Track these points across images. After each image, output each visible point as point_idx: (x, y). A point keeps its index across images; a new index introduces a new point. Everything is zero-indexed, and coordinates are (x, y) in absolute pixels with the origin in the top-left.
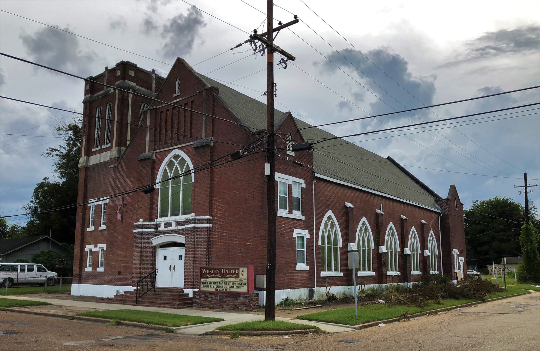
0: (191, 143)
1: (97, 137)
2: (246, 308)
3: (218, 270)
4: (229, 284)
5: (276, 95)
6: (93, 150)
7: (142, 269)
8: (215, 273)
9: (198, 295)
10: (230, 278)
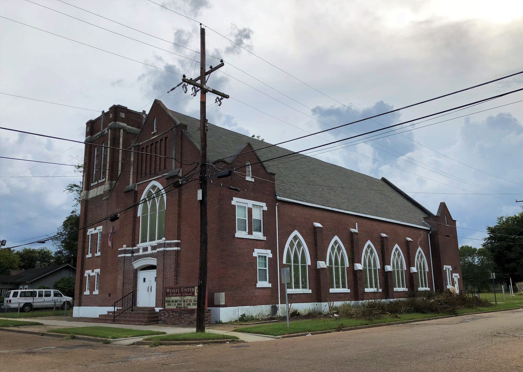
1: (95, 174)
6: (92, 185)
10: (188, 296)
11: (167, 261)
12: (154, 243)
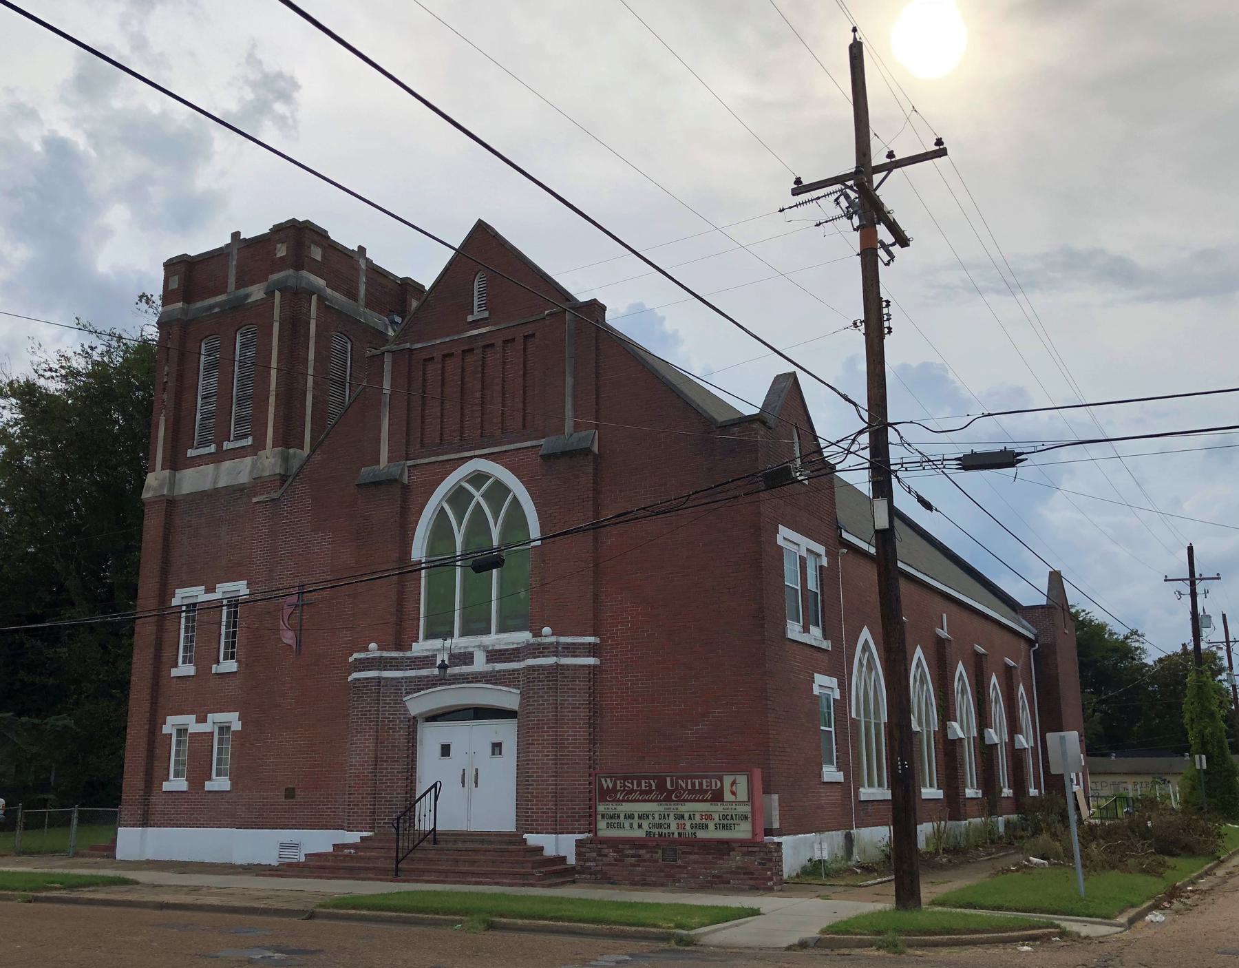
0: (534, 443)
1: (203, 419)
2: (752, 882)
3: (652, 781)
4: (690, 818)
5: (890, 329)
6: (191, 453)
7: (379, 780)
8: (643, 788)
9: (592, 850)
10: (694, 801)
11: (564, 696)
12: (496, 639)
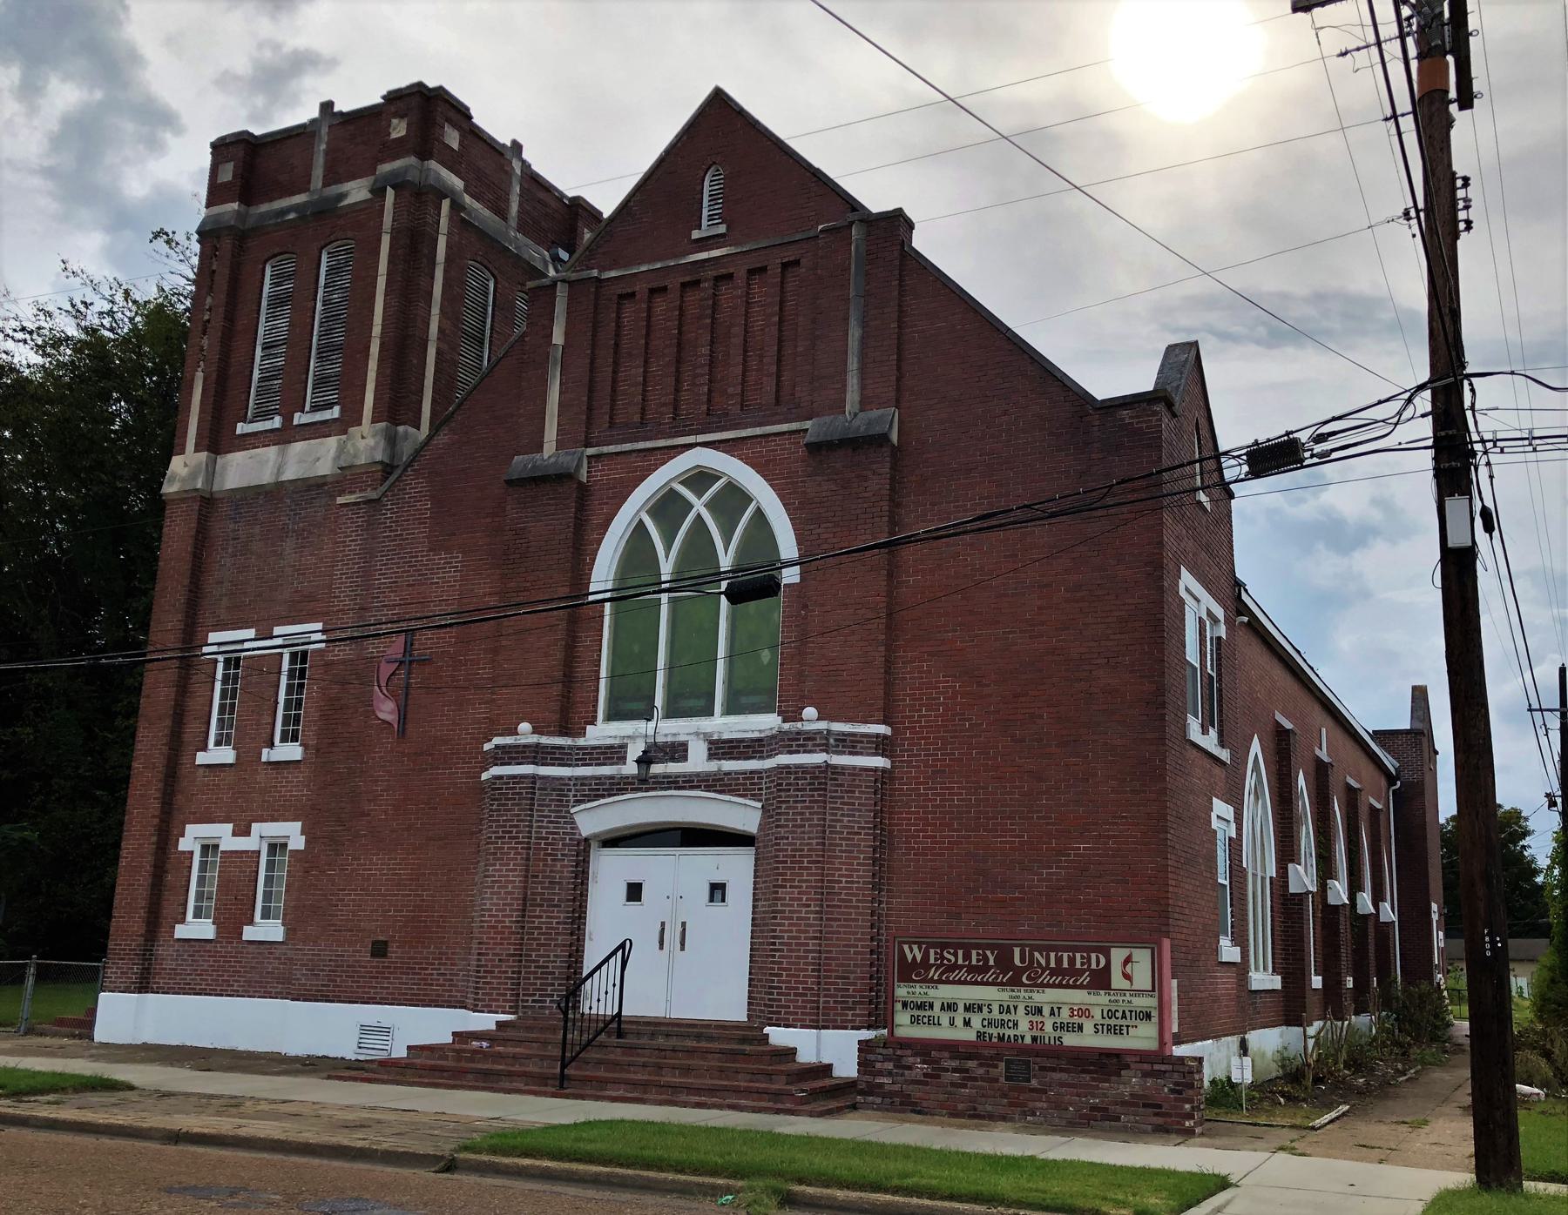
0: (794, 426)
1: (261, 380)
2: (1160, 1120)
3: (988, 953)
4: (1052, 1013)
5: (1469, 224)
6: (241, 428)
7: (528, 933)
9: (887, 1059)
10: (1060, 986)
11: (836, 815)
12: (724, 725)
